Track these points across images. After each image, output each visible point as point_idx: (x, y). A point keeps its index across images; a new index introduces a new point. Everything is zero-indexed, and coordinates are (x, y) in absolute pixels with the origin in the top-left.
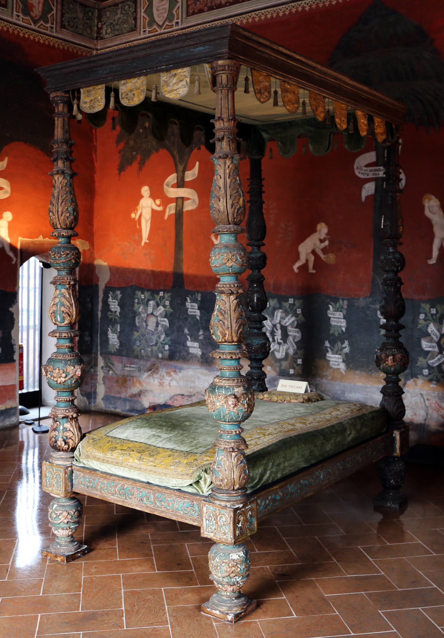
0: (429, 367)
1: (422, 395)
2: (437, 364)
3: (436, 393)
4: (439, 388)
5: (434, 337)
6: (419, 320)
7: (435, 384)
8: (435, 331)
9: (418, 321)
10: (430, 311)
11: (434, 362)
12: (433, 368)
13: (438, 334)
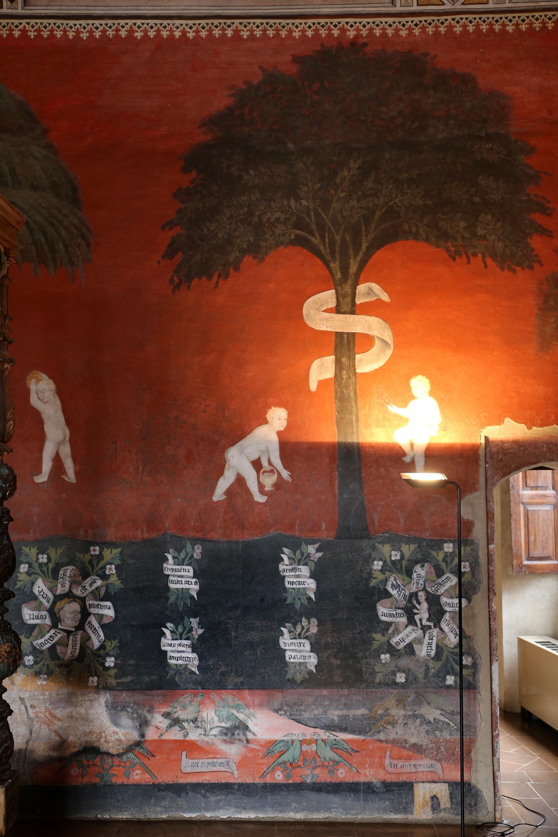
0: (35, 652)
1: (22, 700)
2: (48, 645)
3: (47, 693)
4: (52, 685)
5: (44, 601)
6: (19, 575)
7: (45, 680)
8: (46, 591)
9: (17, 577)
10: (37, 559)
11: (43, 642)
12: (42, 652)
13: (50, 595)
